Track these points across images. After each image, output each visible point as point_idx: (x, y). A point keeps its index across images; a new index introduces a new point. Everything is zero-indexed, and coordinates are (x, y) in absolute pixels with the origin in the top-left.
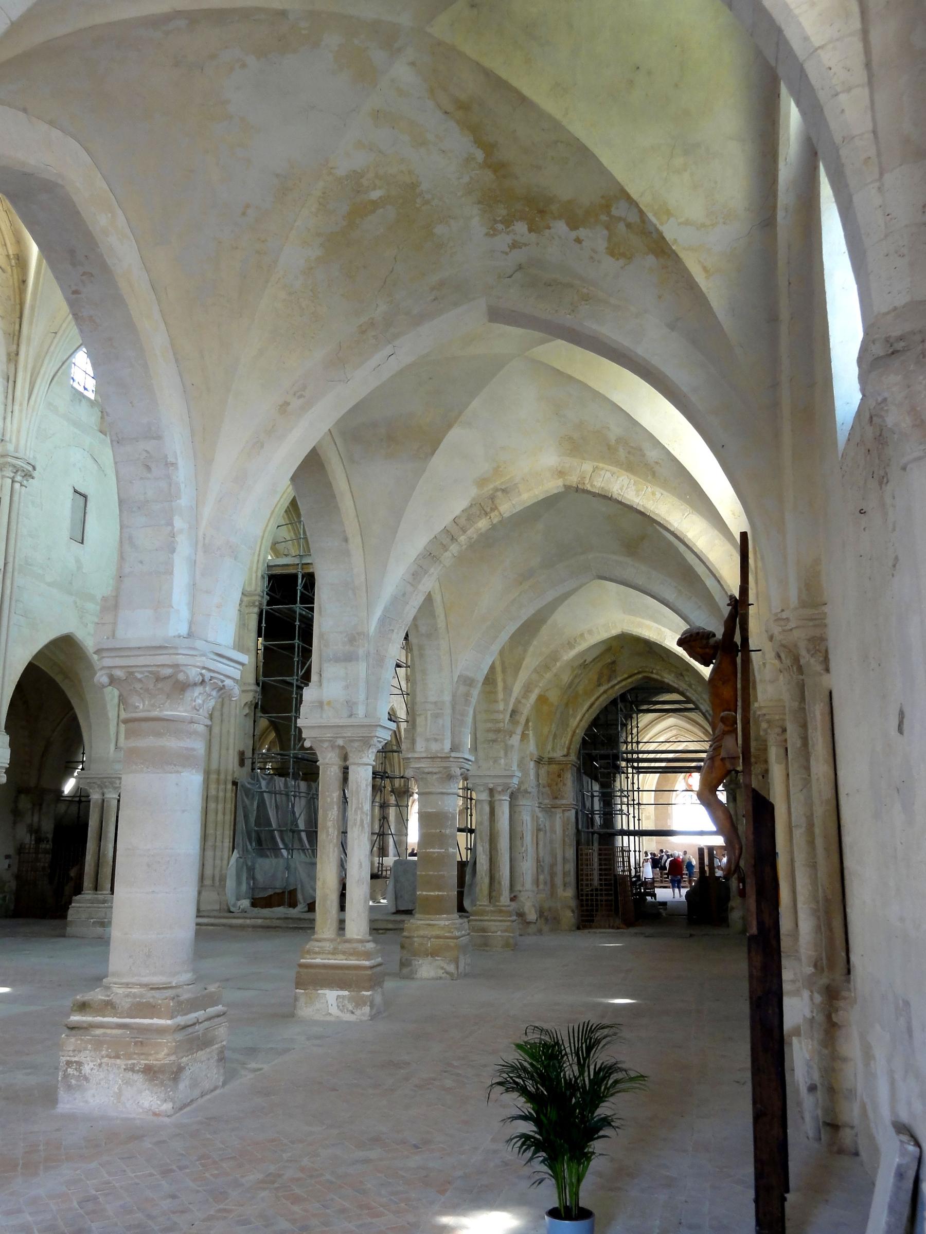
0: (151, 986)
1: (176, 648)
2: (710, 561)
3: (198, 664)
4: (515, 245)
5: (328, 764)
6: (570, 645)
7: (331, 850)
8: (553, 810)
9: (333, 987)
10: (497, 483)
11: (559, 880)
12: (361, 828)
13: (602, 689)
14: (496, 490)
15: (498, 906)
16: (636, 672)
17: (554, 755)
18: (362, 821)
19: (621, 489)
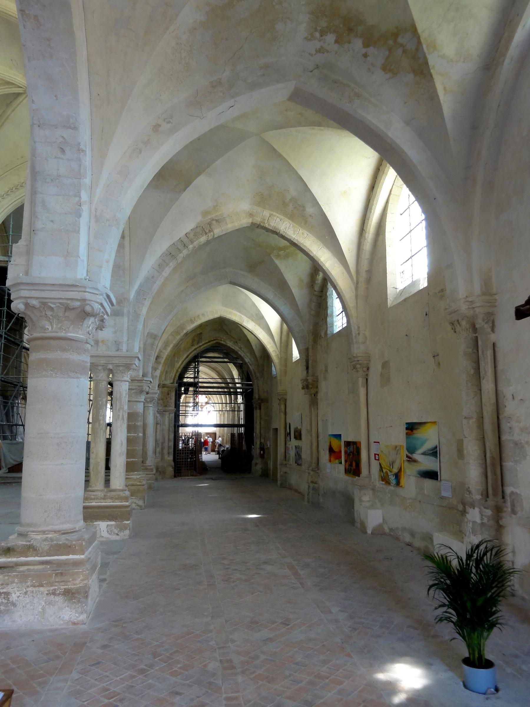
0: (63, 532)
1: (85, 287)
2: (332, 276)
3: (98, 301)
4: (320, 51)
5: (100, 380)
6: (192, 322)
7: (102, 434)
8: (164, 413)
9: (104, 520)
10: (213, 216)
11: (166, 451)
12: (122, 421)
13: (194, 348)
14: (213, 220)
15: (145, 466)
16: (212, 339)
17: (166, 383)
18: (123, 416)
19: (285, 229)
